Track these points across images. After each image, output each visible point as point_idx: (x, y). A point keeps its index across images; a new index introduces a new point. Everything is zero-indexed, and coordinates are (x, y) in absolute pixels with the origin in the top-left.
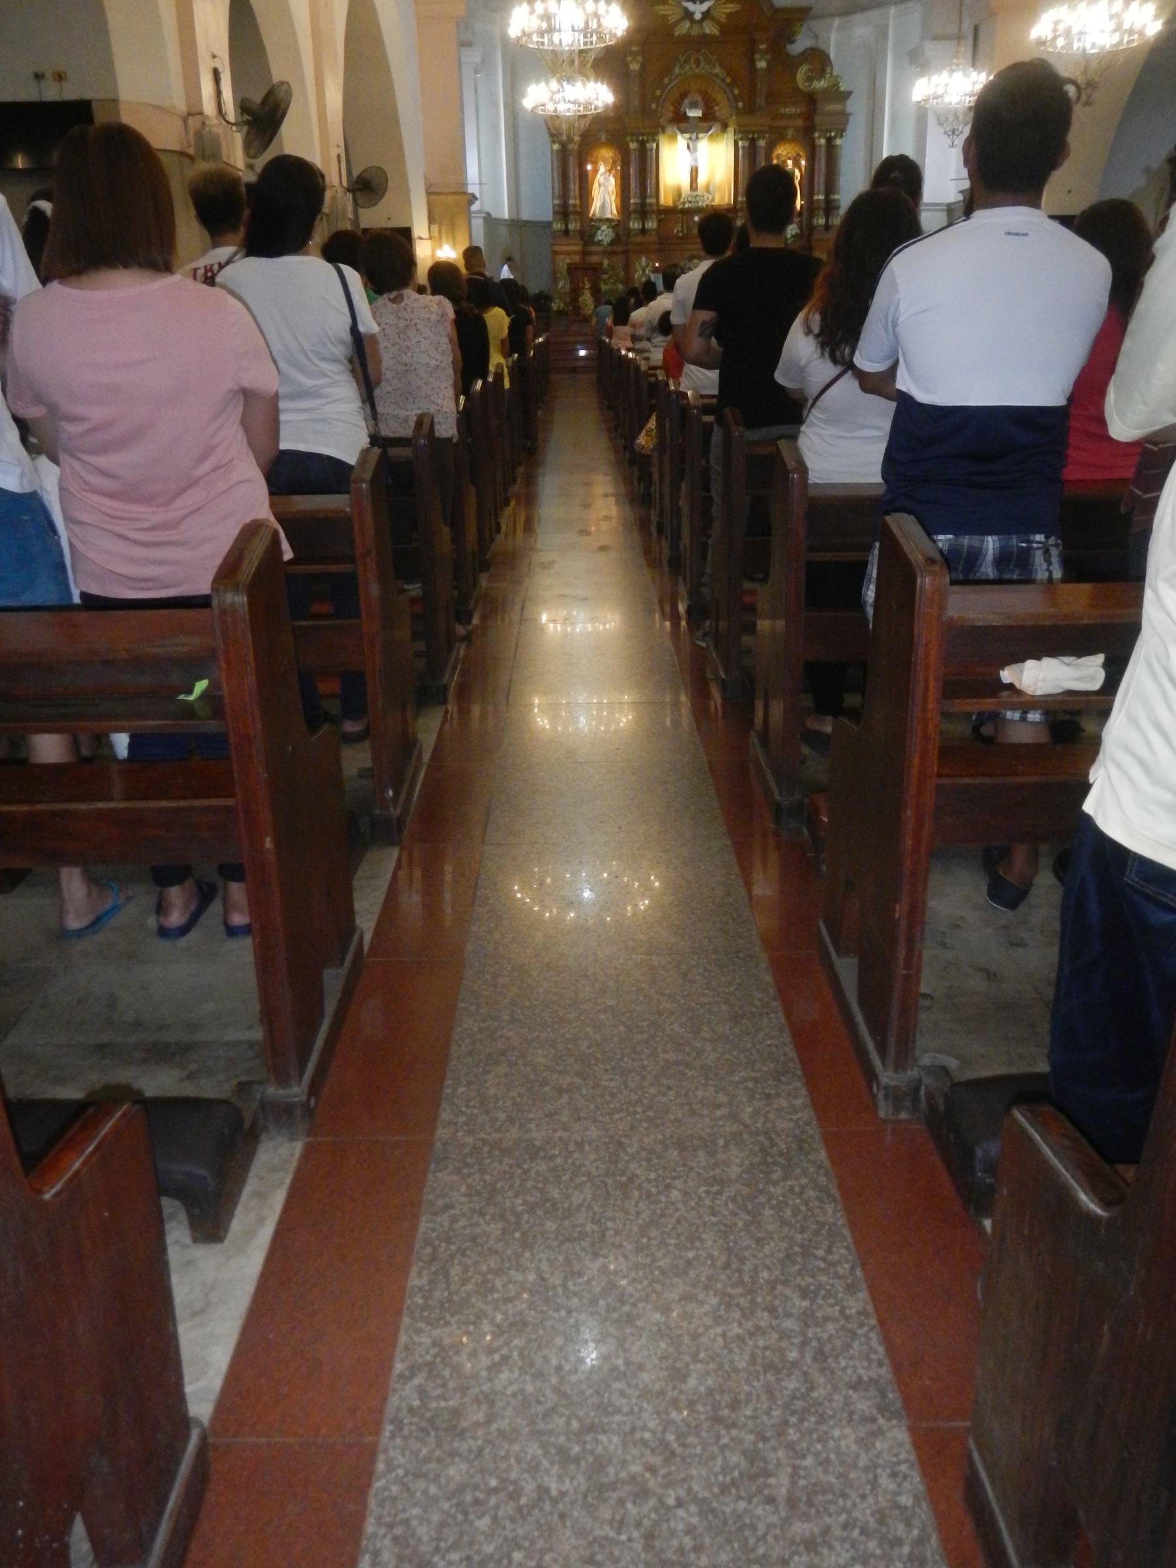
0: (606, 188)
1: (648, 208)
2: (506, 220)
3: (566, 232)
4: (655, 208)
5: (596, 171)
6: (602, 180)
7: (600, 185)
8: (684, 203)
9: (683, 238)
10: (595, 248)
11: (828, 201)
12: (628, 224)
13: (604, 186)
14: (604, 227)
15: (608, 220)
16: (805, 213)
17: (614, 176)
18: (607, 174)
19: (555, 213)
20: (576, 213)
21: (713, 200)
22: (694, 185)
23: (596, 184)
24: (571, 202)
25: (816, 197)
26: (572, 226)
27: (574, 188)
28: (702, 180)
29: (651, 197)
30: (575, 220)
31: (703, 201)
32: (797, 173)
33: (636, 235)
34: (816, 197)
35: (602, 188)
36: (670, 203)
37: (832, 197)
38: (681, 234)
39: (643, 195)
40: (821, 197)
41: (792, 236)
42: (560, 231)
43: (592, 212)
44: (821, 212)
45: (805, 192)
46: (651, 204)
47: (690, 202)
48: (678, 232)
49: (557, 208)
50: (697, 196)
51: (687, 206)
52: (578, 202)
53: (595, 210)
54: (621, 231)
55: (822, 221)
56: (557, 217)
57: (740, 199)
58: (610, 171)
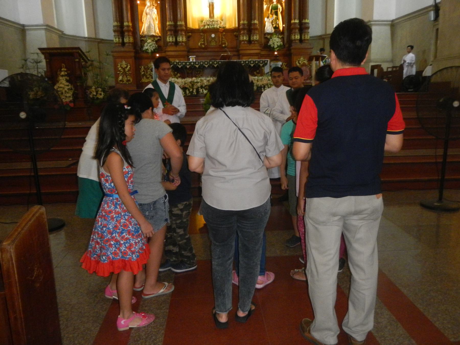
0: (151, 15)
1: (179, 28)
2: (85, 38)
3: (123, 44)
4: (184, 28)
5: (145, 5)
6: (148, 11)
7: (147, 14)
8: (205, 26)
9: (203, 48)
10: (145, 55)
11: (301, 23)
12: (166, 38)
13: (149, 14)
14: (149, 41)
15: (153, 36)
16: (286, 34)
17: (156, 8)
18: (152, 7)
19: (115, 31)
20: (128, 31)
21: (225, 24)
22: (212, 15)
23: (144, 14)
24: (126, 24)
25: (293, 21)
26: (126, 40)
27: (127, 15)
28: (217, 14)
29: (181, 20)
30: (129, 35)
31: (217, 25)
32: (279, 6)
33: (171, 45)
34: (293, 21)
35: (148, 16)
36: (197, 27)
37: (304, 21)
38: (203, 46)
39: (175, 19)
40: (297, 21)
41: (278, 47)
42: (119, 43)
43: (142, 32)
44: (297, 31)
45: (286, 18)
46: (181, 25)
47: (209, 25)
48: (201, 44)
49: (116, 28)
50: (213, 21)
51: (206, 27)
52: (130, 24)
53: (144, 29)
54: (162, 43)
55: (298, 37)
56: (116, 34)
57: (242, 22)
58: (153, 5)
